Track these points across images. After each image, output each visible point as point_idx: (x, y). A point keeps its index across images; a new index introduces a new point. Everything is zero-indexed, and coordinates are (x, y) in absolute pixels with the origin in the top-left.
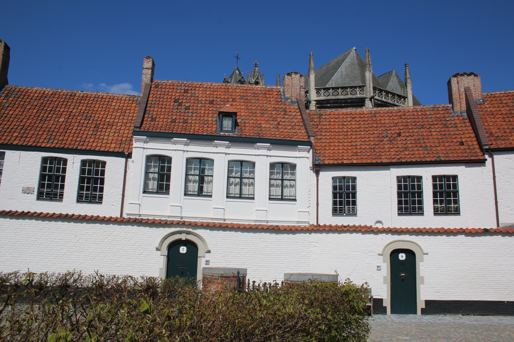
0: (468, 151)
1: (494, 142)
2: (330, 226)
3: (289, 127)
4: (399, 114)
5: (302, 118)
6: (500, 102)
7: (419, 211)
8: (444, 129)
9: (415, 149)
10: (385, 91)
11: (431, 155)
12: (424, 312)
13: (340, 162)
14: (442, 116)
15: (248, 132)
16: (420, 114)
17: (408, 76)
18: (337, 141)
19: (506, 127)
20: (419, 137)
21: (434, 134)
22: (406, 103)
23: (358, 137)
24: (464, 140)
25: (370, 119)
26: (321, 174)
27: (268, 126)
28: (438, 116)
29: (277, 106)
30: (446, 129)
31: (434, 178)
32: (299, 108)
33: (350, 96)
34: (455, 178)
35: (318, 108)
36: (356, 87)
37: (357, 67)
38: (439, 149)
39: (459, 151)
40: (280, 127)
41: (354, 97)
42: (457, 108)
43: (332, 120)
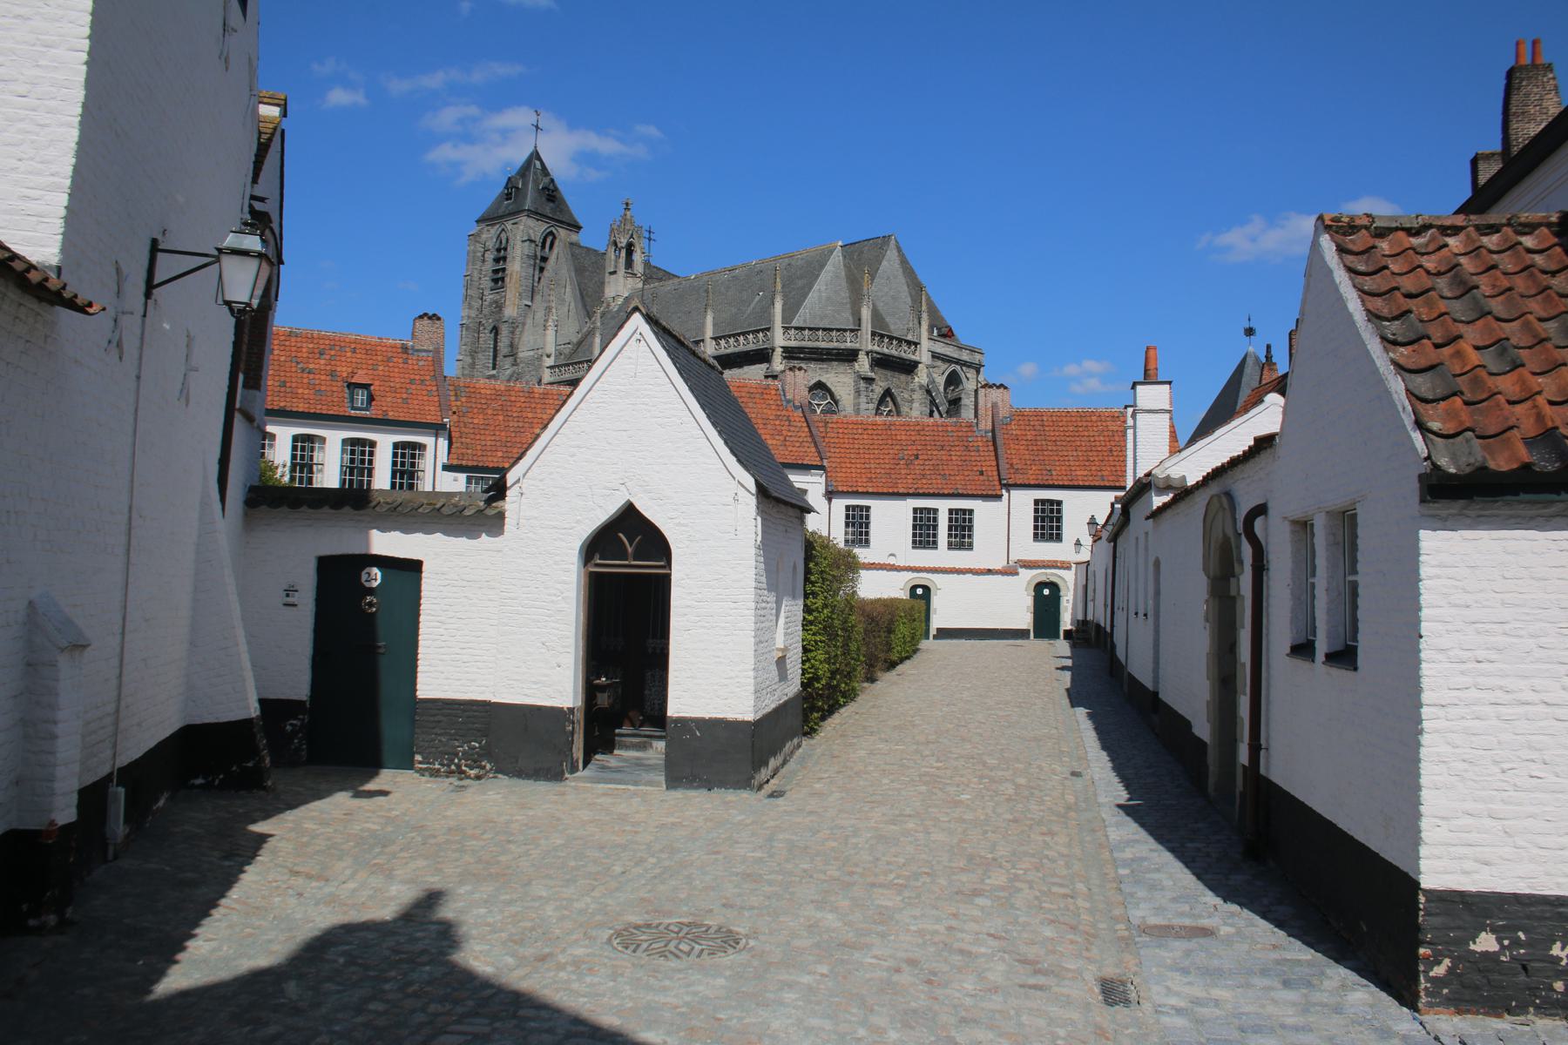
0: (987, 483)
3: (798, 444)
5: (810, 431)
9: (933, 477)
10: (888, 337)
11: (950, 486)
12: (935, 637)
13: (855, 489)
16: (940, 429)
17: (924, 308)
19: (1027, 457)
21: (954, 458)
22: (917, 353)
23: (872, 456)
26: (834, 501)
27: (774, 442)
28: (960, 434)
30: (968, 453)
31: (951, 511)
33: (835, 345)
34: (971, 512)
35: (785, 358)
36: (845, 330)
37: (844, 283)
40: (787, 443)
41: (843, 346)
42: (982, 426)
43: (841, 431)
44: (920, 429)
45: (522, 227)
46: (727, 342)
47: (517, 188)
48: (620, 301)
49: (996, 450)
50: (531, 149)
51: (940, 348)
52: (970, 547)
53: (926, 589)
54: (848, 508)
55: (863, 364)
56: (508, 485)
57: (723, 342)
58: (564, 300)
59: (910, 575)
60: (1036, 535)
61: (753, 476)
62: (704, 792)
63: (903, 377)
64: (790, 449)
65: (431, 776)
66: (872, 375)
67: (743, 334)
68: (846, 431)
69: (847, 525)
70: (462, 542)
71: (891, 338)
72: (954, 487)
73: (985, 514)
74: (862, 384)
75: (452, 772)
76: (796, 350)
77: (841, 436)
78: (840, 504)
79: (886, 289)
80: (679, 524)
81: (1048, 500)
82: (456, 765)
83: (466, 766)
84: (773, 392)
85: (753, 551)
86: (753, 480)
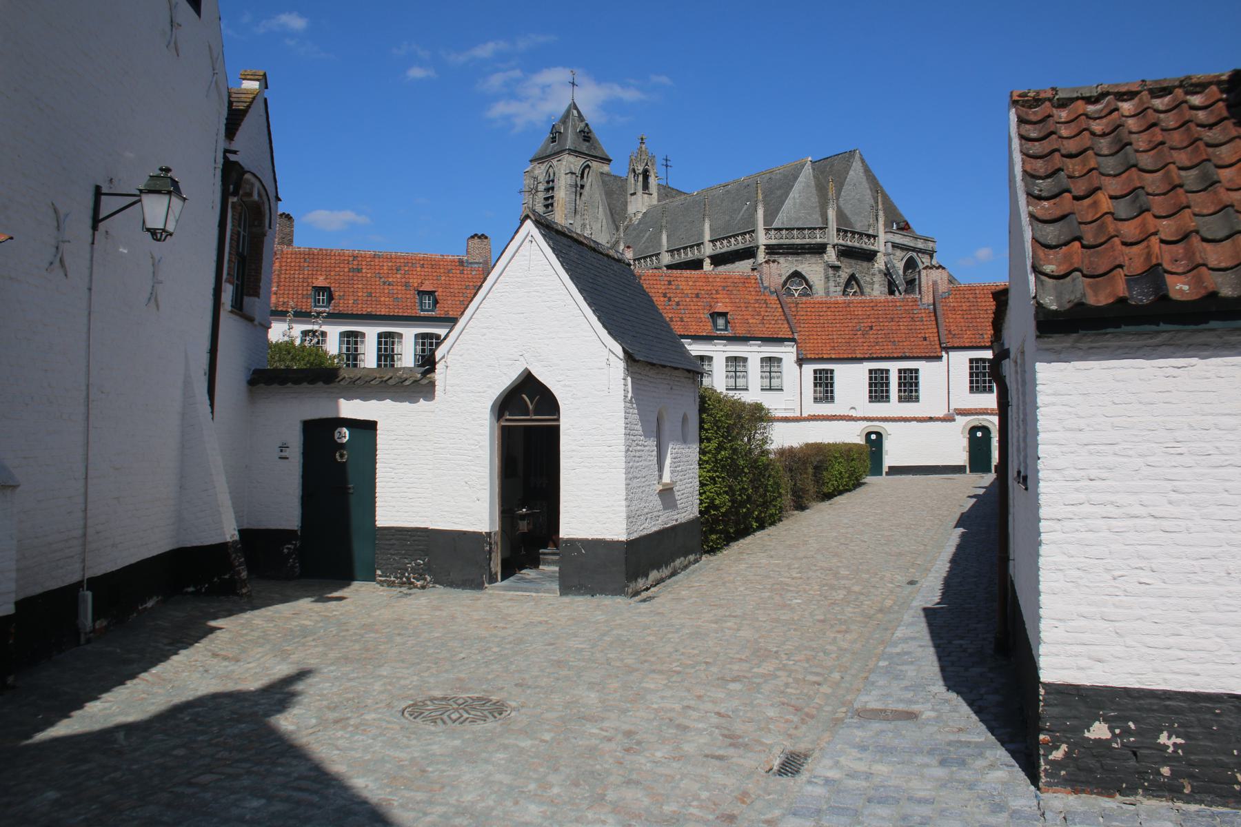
0: (929, 347)
1: (951, 340)
2: (823, 415)
3: (773, 322)
4: (871, 305)
5: (783, 311)
6: (962, 296)
7: (886, 399)
8: (911, 323)
10: (851, 232)
11: (898, 351)
12: (887, 474)
13: (821, 356)
14: (911, 308)
15: (741, 331)
17: (880, 207)
18: (815, 333)
19: (963, 324)
20: (889, 331)
21: (902, 328)
22: (876, 244)
23: (835, 329)
24: (927, 336)
25: (844, 309)
26: (804, 366)
27: (754, 321)
28: (907, 308)
29: (758, 298)
31: (900, 371)
32: (779, 299)
33: (807, 241)
34: (917, 371)
35: (767, 253)
36: (815, 229)
37: (814, 191)
38: (905, 344)
39: (922, 347)
41: (813, 241)
42: (925, 300)
43: (809, 310)
44: (874, 305)
45: (564, 163)
46: (722, 244)
47: (560, 133)
48: (640, 216)
49: (936, 320)
50: (571, 101)
51: (898, 239)
52: (917, 399)
53: (879, 435)
54: (815, 371)
55: (831, 255)
56: (437, 360)
57: (718, 244)
58: (598, 218)
59: (866, 424)
60: (971, 389)
61: (621, 345)
62: (588, 597)
63: (865, 264)
64: (767, 326)
65: (388, 586)
66: (838, 263)
67: (734, 236)
68: (813, 310)
69: (815, 385)
70: (406, 406)
71: (853, 233)
72: (902, 351)
73: (928, 371)
74: (831, 272)
75: (405, 583)
76: (776, 247)
77: (809, 314)
78: (809, 369)
79: (853, 194)
80: (565, 386)
81: (981, 359)
82: (406, 577)
83: (414, 578)
84: (753, 281)
85: (621, 405)
86: (621, 348)
